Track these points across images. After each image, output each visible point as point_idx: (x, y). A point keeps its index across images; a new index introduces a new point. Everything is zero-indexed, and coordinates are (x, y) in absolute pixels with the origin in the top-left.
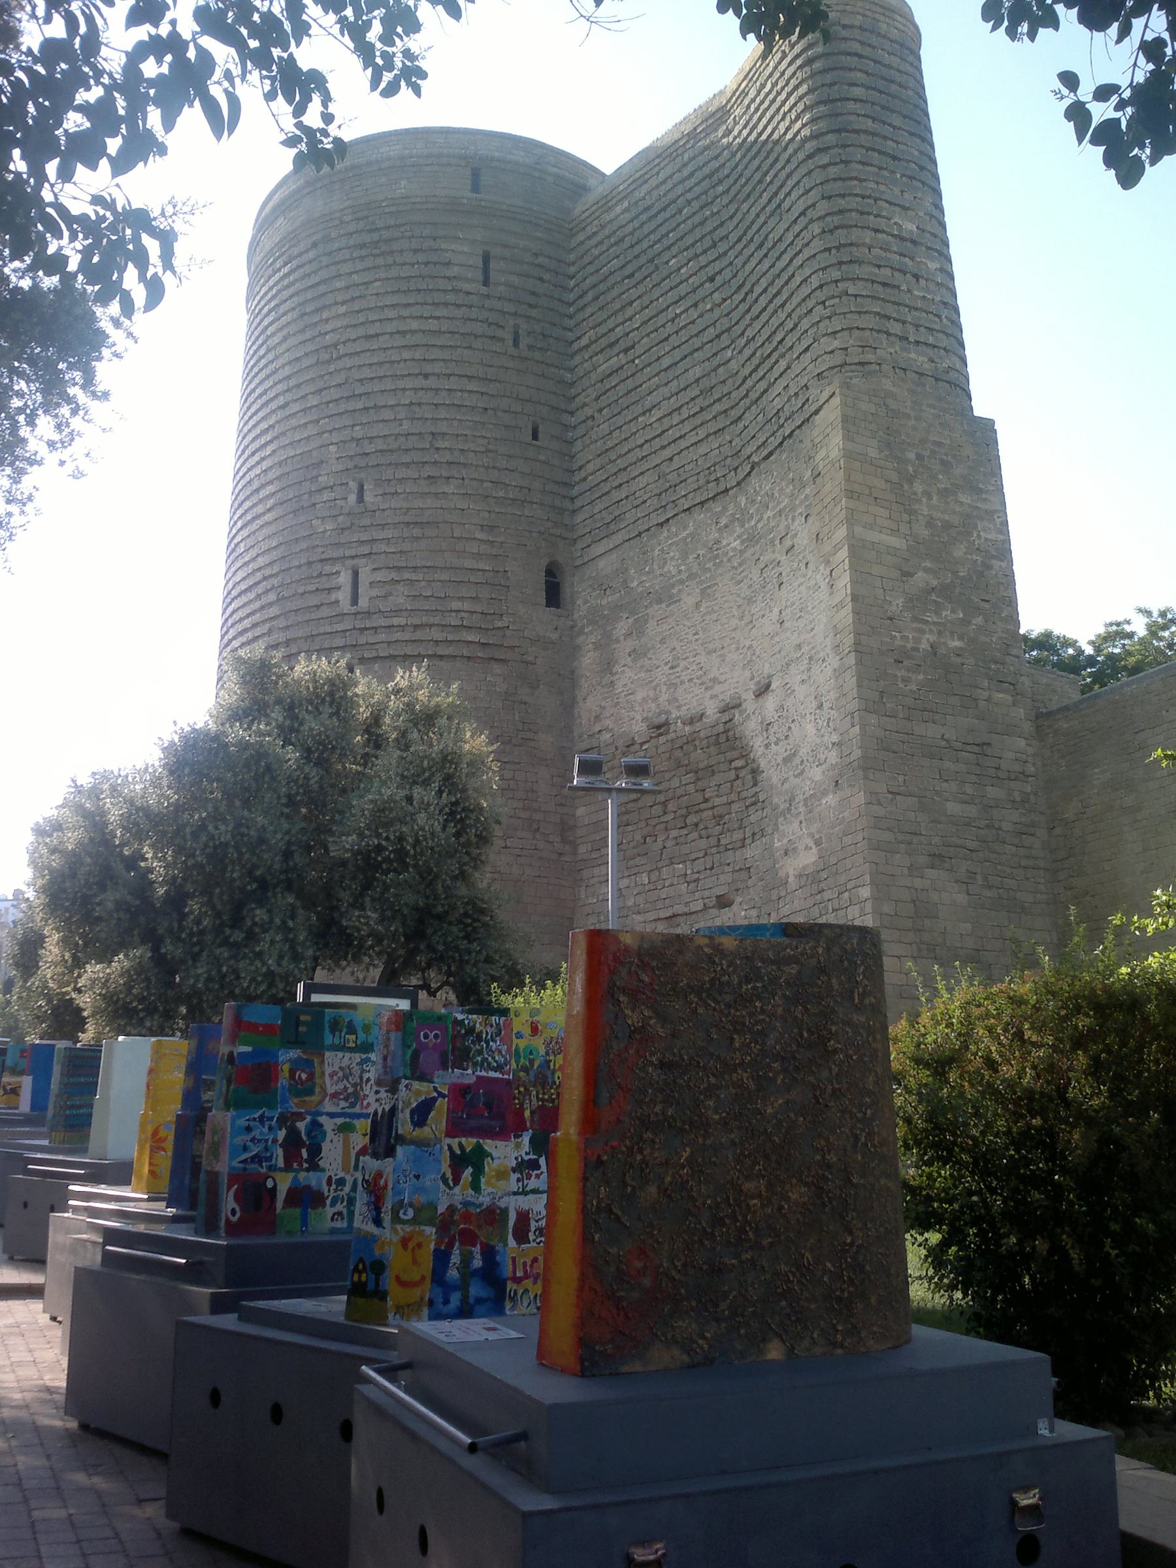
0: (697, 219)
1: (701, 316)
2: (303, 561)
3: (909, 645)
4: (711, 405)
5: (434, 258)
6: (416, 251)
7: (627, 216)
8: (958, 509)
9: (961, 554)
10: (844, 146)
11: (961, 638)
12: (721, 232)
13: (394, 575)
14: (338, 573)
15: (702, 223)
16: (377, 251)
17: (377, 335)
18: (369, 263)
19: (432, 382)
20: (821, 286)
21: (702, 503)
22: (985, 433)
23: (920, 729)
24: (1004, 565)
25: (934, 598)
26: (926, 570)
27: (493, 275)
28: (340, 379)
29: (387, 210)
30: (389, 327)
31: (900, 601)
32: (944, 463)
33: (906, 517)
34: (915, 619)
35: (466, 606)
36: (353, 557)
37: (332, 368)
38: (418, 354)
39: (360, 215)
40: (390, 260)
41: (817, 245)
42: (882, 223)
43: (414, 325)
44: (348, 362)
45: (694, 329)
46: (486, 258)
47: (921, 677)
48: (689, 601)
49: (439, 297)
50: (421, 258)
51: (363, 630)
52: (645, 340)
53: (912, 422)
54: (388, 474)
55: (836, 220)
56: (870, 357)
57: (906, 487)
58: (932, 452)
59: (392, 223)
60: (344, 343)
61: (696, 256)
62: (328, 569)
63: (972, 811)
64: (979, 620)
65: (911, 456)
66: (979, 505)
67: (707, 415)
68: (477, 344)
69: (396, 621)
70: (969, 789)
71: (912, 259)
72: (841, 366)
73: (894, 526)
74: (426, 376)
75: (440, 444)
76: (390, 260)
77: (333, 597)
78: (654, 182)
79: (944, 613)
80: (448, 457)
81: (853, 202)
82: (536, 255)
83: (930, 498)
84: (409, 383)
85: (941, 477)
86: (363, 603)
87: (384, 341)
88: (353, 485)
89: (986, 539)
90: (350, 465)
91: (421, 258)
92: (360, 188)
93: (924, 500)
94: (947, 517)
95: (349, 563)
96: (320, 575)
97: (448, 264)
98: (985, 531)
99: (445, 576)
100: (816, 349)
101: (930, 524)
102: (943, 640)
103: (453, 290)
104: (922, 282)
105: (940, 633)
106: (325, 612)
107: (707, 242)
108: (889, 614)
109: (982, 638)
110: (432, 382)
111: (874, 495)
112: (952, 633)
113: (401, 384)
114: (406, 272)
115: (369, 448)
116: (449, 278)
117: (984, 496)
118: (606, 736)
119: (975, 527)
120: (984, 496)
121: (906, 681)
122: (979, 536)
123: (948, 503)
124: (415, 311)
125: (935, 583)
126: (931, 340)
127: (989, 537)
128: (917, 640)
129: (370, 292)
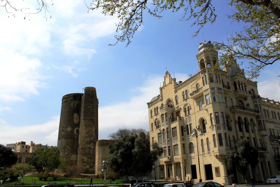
46: (74, 104)
63: (88, 152)
70: (88, 150)
101: (88, 131)
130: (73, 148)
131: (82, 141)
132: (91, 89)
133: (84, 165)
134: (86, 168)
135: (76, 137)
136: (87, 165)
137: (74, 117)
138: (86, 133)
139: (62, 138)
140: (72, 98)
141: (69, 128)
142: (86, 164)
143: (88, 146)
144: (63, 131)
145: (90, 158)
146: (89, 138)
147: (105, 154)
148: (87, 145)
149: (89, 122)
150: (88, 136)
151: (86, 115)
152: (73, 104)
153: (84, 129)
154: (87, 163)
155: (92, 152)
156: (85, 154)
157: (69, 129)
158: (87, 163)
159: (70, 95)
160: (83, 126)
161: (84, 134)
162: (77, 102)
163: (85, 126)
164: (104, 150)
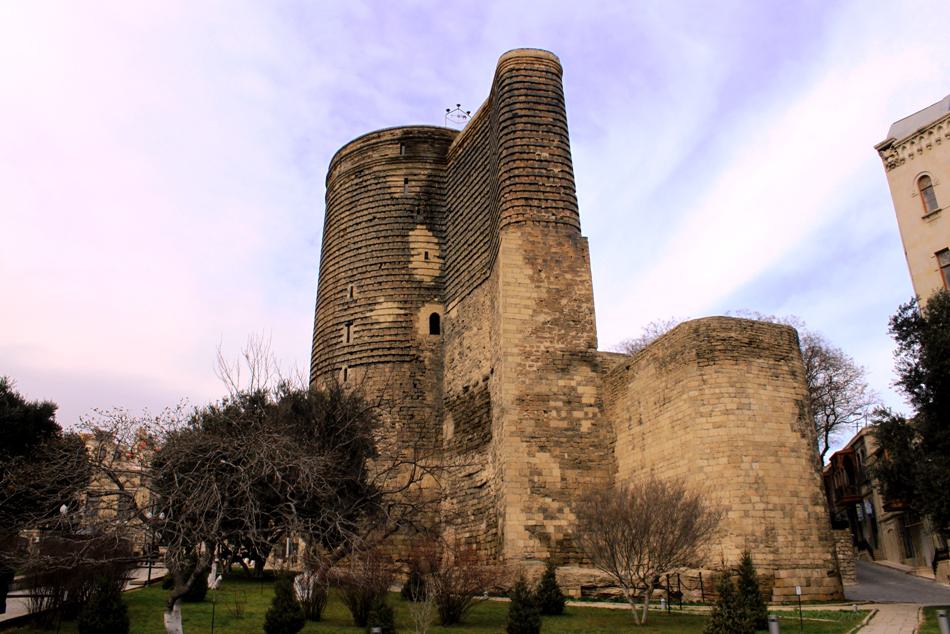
6: (376, 184)
10: (515, 124)
13: (364, 328)
19: (381, 240)
20: (503, 189)
21: (480, 284)
22: (581, 246)
24: (589, 305)
26: (546, 313)
27: (408, 189)
30: (365, 219)
34: (538, 337)
35: (394, 338)
38: (375, 229)
41: (503, 170)
42: (531, 156)
44: (349, 236)
46: (406, 181)
47: (540, 364)
48: (475, 329)
49: (384, 203)
50: (379, 186)
51: (351, 353)
53: (542, 245)
55: (507, 160)
56: (520, 218)
63: (564, 424)
64: (574, 333)
65: (540, 261)
67: (482, 244)
68: (399, 220)
69: (363, 348)
71: (546, 169)
72: (509, 224)
74: (379, 238)
77: (339, 340)
80: (386, 272)
81: (516, 149)
82: (429, 176)
83: (548, 278)
84: (371, 242)
86: (351, 342)
90: (348, 280)
91: (379, 186)
97: (389, 187)
98: (579, 290)
100: (503, 216)
101: (549, 291)
104: (551, 180)
105: (551, 342)
110: (381, 240)
114: (371, 193)
115: (355, 272)
116: (390, 193)
118: (451, 393)
121: (530, 366)
125: (549, 319)
128: (539, 347)
130: (412, 416)
132: (538, 59)
133: (544, 510)
134: (559, 528)
135: (428, 354)
136: (560, 510)
137: (412, 246)
139: (344, 367)
140: (393, 151)
141: (385, 305)
142: (555, 505)
143: (561, 383)
144: (349, 324)
145: (578, 464)
146: (561, 338)
147: (752, 418)
148: (552, 376)
149: (551, 241)
150: (555, 322)
151: (526, 195)
152: (401, 184)
153: (529, 281)
154: (562, 495)
155: (585, 426)
156: (543, 440)
157: (386, 312)
158: (562, 495)
159: (379, 137)
160: (519, 259)
161: (526, 307)
162: (423, 171)
163: (530, 260)
164: (741, 392)
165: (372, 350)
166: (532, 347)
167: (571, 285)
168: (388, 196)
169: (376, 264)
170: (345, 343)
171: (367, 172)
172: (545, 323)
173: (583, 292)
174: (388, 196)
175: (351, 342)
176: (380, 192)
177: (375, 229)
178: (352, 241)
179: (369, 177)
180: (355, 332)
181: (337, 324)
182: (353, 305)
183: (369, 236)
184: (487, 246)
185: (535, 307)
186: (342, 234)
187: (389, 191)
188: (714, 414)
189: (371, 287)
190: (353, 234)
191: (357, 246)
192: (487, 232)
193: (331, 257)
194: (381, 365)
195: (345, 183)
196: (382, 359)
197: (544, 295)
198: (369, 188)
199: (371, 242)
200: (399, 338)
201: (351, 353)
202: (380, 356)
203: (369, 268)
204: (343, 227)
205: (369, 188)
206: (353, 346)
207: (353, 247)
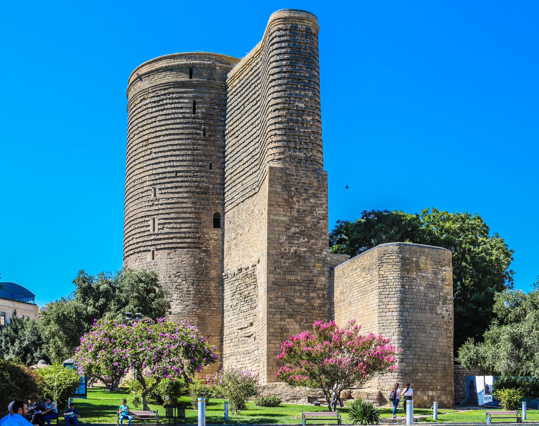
0: (253, 92)
1: (253, 129)
2: (140, 216)
3: (287, 252)
4: (254, 162)
5: (177, 105)
7: (238, 85)
8: (309, 205)
9: (309, 220)
11: (306, 247)
12: (258, 99)
14: (149, 220)
15: (254, 94)
16: (158, 104)
17: (159, 136)
18: (157, 109)
23: (288, 277)
25: (297, 235)
26: (295, 227)
28: (149, 152)
29: (162, 88)
30: (163, 133)
31: (285, 238)
32: (305, 189)
33: (289, 210)
34: (289, 243)
35: (187, 230)
36: (154, 215)
37: (146, 148)
38: (171, 143)
39: (154, 90)
40: (163, 108)
43: (170, 132)
45: (252, 133)
46: (194, 103)
49: (178, 121)
50: (173, 106)
52: (241, 134)
54: (163, 186)
57: (290, 200)
58: (302, 186)
59: (163, 93)
60: (150, 139)
61: (253, 106)
62: (147, 219)
64: (313, 241)
65: (293, 189)
66: (318, 202)
67: (252, 166)
73: (285, 213)
75: (179, 174)
76: (163, 108)
77: (148, 229)
78: (245, 73)
79: (300, 240)
80: (181, 179)
83: (299, 202)
84: (169, 153)
85: (304, 195)
87: (162, 138)
88: (153, 190)
89: (319, 214)
90: (152, 183)
92: (154, 79)
93: (297, 203)
94: (305, 208)
95: (152, 217)
96: (144, 221)
99: (180, 221)
101: (298, 211)
102: (299, 249)
103: (183, 117)
105: (298, 247)
106: (146, 233)
107: (255, 102)
108: (280, 242)
109: (314, 247)
111: (278, 204)
112: (303, 246)
113: (166, 154)
115: (157, 177)
116: (182, 113)
117: (320, 199)
119: (315, 210)
120: (320, 199)
121: (284, 263)
122: (316, 213)
123: (305, 203)
124: (171, 127)
125: (298, 230)
126: (305, 146)
127: (320, 213)
128: (290, 250)
129: (157, 120)
131: (274, 252)
138: (293, 220)
150: (302, 233)
153: (284, 204)
165: (172, 238)
166: (285, 250)
167: (313, 207)
168: (180, 116)
169: (173, 172)
170: (151, 232)
171: (163, 92)
172: (295, 233)
173: (322, 212)
174: (180, 116)
175: (156, 231)
176: (174, 111)
177: (171, 143)
178: (154, 151)
179: (165, 97)
180: (159, 224)
181: (145, 216)
182: (157, 203)
183: (166, 149)
184: (256, 168)
185: (288, 223)
186: (144, 143)
187: (181, 111)
188: (390, 303)
189: (170, 190)
190: (154, 145)
191: (157, 155)
192: (257, 157)
193: (137, 162)
194: (179, 250)
195: (144, 99)
196: (179, 245)
197: (295, 214)
198: (166, 107)
199: (169, 153)
200: (191, 230)
201: (156, 240)
202: (178, 243)
203: (168, 175)
204: (146, 137)
205: (166, 107)
206: (158, 234)
207: (154, 156)
